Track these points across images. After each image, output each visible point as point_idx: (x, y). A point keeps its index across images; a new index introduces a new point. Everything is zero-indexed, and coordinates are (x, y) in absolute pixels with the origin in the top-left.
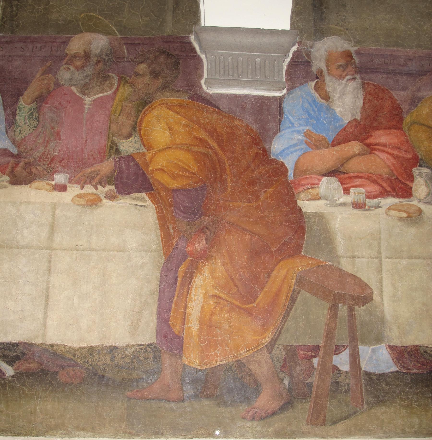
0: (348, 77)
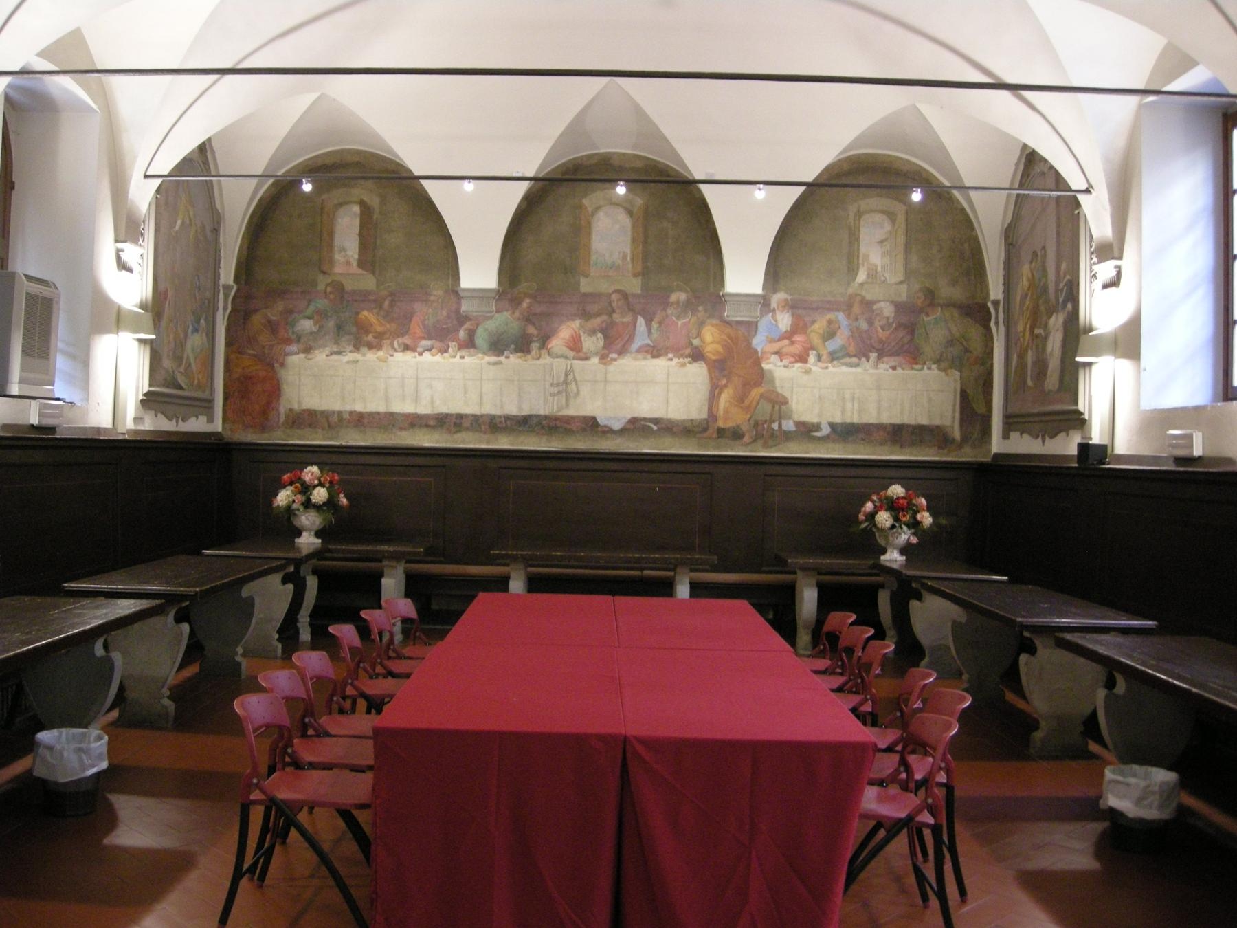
0: (786, 311)
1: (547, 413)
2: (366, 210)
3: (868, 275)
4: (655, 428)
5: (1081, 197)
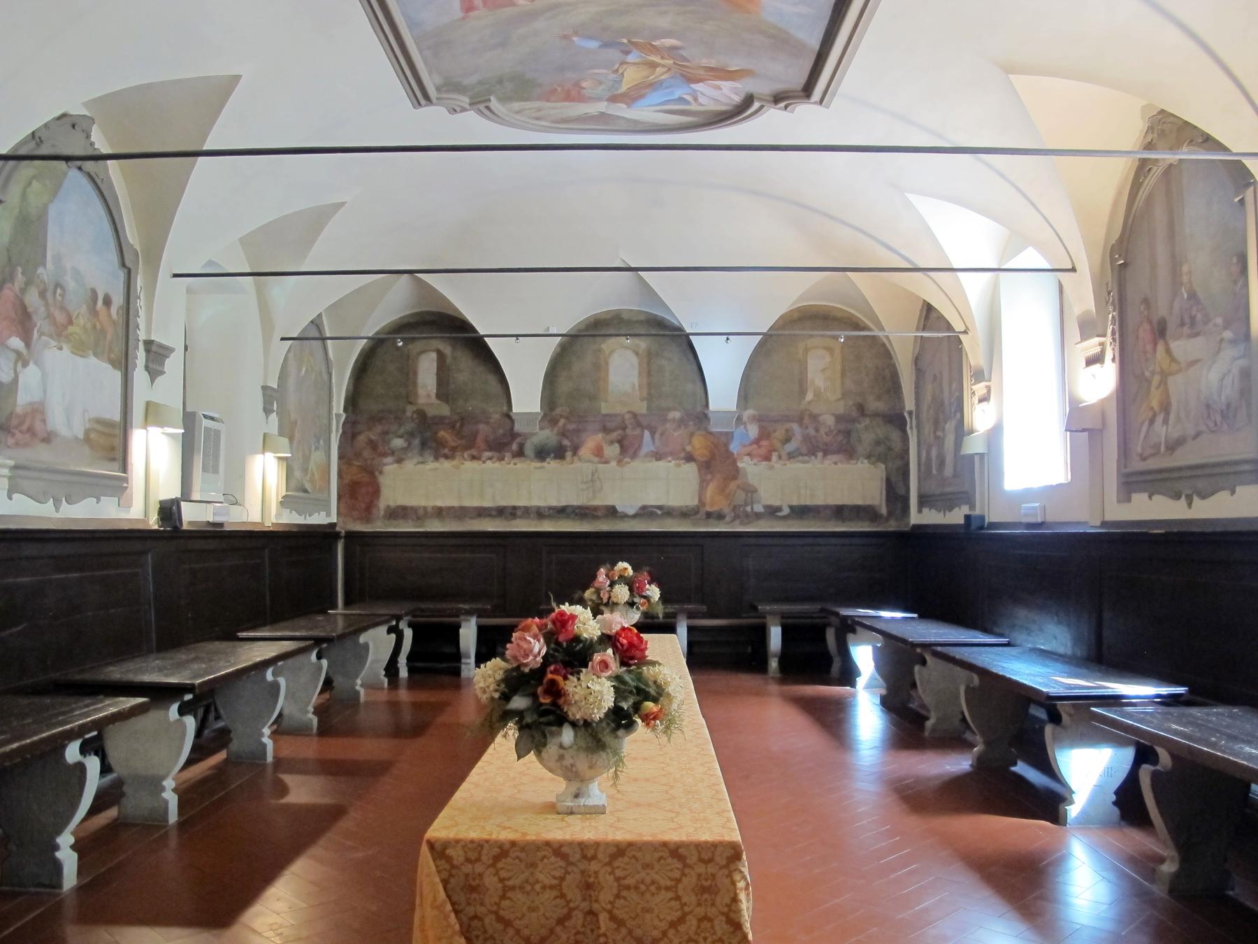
1: (579, 504)
2: (441, 356)
3: (815, 395)
4: (659, 512)
5: (962, 337)
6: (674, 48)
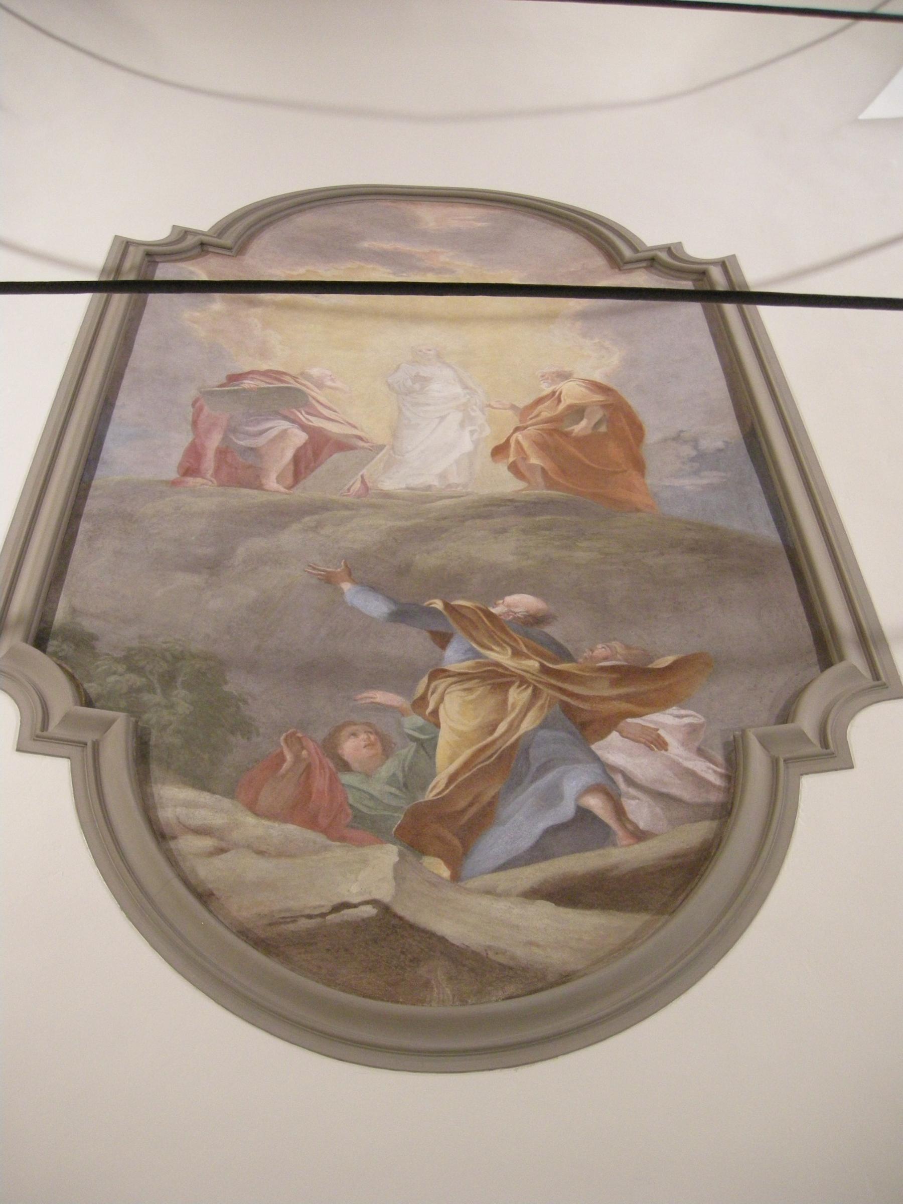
6: (535, 620)
